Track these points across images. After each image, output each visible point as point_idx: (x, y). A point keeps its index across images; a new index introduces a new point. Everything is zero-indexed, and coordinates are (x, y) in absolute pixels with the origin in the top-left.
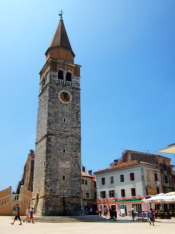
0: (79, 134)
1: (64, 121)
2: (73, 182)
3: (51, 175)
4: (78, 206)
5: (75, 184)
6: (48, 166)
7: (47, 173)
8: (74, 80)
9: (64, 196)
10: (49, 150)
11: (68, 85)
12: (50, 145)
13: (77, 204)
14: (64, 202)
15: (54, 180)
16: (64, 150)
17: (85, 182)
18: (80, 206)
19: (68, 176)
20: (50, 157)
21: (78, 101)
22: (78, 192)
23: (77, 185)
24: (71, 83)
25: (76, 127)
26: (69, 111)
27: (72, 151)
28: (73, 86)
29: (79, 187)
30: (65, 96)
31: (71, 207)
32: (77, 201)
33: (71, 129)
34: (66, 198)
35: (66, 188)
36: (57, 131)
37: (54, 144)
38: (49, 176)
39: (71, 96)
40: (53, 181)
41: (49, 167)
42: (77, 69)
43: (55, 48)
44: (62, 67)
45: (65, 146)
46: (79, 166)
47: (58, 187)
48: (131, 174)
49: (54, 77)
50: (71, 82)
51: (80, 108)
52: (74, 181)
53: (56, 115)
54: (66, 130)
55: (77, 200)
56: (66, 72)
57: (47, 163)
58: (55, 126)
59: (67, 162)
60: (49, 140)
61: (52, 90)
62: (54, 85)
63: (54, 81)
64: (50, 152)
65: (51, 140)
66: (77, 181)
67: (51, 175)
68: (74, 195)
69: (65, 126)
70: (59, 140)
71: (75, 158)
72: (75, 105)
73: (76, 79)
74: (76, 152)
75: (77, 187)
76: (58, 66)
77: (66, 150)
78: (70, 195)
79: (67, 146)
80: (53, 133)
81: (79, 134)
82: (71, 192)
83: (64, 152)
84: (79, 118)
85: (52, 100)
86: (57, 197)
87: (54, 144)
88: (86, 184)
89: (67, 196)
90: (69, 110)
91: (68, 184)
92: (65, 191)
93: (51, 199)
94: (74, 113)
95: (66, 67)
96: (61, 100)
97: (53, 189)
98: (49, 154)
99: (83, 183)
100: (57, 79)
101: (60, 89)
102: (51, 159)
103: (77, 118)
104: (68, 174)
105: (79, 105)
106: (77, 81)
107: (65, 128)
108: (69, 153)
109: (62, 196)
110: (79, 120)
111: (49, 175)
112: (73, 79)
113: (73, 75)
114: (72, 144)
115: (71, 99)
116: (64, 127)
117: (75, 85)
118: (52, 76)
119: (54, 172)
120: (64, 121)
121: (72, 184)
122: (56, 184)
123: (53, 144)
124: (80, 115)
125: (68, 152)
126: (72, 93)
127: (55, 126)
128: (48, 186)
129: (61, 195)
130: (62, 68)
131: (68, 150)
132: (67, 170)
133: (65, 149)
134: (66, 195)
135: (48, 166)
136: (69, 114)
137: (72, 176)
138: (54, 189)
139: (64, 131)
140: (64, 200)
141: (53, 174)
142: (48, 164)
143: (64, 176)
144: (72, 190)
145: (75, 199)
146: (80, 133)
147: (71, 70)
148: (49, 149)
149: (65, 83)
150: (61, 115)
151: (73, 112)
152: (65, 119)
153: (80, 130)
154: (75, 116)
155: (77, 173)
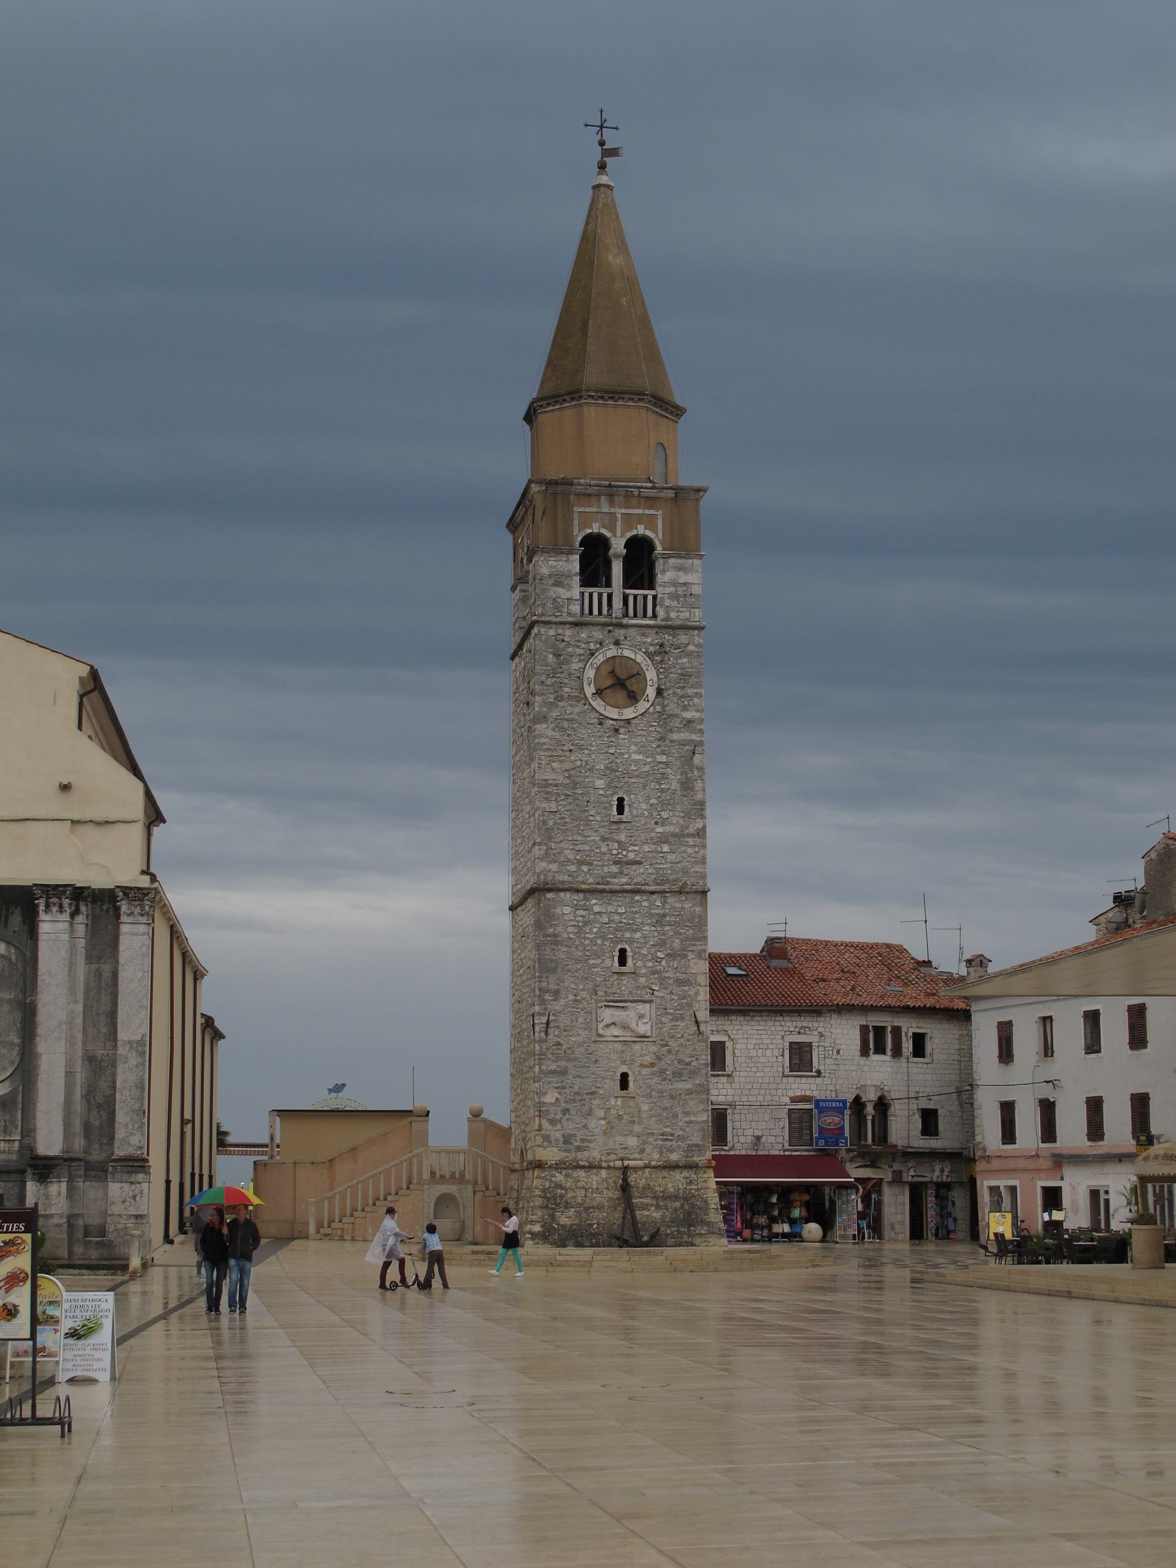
0: (698, 868)
1: (620, 810)
2: (666, 1103)
3: (563, 1072)
5: (679, 1110)
6: (547, 1034)
7: (544, 1067)
8: (669, 576)
9: (626, 1163)
10: (551, 961)
11: (635, 615)
12: (555, 936)
13: (741, 1195)
14: (625, 1188)
15: (578, 1094)
16: (623, 952)
17: (907, 1046)
19: (645, 1071)
21: (690, 691)
22: (697, 1145)
23: (686, 1114)
24: (655, 597)
25: (683, 836)
26: (641, 757)
27: (660, 955)
28: (661, 613)
29: (698, 1122)
31: (658, 1207)
32: (691, 1183)
33: (653, 847)
34: (636, 1169)
35: (638, 1129)
36: (585, 868)
37: (570, 929)
39: (651, 674)
40: (574, 1101)
43: (565, 400)
45: (628, 935)
46: (697, 1022)
47: (597, 1125)
48: (1131, 1008)
49: (558, 584)
52: (672, 1097)
53: (575, 785)
54: (631, 856)
55: (686, 1178)
56: (623, 542)
57: (544, 1020)
58: (575, 843)
62: (560, 631)
64: (554, 970)
65: (558, 911)
66: (689, 1092)
67: (563, 1072)
68: (674, 1157)
69: (622, 837)
70: (597, 909)
71: (678, 990)
72: (677, 716)
73: (680, 568)
75: (690, 1122)
76: (576, 516)
77: (629, 954)
78: (656, 1156)
79: (638, 935)
80: (566, 878)
81: (698, 868)
82: (661, 1143)
83: (623, 961)
84: (698, 785)
85: (554, 714)
87: (570, 929)
89: (640, 1163)
92: (632, 1142)
93: (567, 1175)
94: (667, 764)
95: (620, 511)
97: (574, 1135)
98: (552, 978)
99: (897, 1052)
100: (576, 591)
101: (592, 646)
102: (562, 1002)
103: (687, 786)
104: (642, 1065)
106: (683, 578)
108: (650, 964)
109: (618, 1164)
110: (699, 796)
111: (553, 1072)
112: (664, 571)
113: (659, 548)
114: (660, 920)
115: (651, 692)
116: (619, 842)
117: (675, 603)
118: (551, 582)
119: (575, 1059)
120: (620, 810)
121: (664, 1109)
122: (590, 1113)
125: (639, 964)
127: (575, 843)
128: (553, 1122)
129: (613, 1157)
130: (604, 526)
131: (644, 952)
132: (637, 1047)
133: (627, 947)
134: (637, 1156)
135: (547, 1034)
136: (647, 768)
137: (662, 1071)
139: (615, 863)
140: (625, 1180)
141: (572, 1072)
142: (548, 1023)
143: (624, 1076)
144: (663, 1135)
145: (679, 1176)
146: (703, 861)
147: (650, 522)
149: (617, 603)
150: (600, 783)
151: (663, 758)
155: (688, 1060)
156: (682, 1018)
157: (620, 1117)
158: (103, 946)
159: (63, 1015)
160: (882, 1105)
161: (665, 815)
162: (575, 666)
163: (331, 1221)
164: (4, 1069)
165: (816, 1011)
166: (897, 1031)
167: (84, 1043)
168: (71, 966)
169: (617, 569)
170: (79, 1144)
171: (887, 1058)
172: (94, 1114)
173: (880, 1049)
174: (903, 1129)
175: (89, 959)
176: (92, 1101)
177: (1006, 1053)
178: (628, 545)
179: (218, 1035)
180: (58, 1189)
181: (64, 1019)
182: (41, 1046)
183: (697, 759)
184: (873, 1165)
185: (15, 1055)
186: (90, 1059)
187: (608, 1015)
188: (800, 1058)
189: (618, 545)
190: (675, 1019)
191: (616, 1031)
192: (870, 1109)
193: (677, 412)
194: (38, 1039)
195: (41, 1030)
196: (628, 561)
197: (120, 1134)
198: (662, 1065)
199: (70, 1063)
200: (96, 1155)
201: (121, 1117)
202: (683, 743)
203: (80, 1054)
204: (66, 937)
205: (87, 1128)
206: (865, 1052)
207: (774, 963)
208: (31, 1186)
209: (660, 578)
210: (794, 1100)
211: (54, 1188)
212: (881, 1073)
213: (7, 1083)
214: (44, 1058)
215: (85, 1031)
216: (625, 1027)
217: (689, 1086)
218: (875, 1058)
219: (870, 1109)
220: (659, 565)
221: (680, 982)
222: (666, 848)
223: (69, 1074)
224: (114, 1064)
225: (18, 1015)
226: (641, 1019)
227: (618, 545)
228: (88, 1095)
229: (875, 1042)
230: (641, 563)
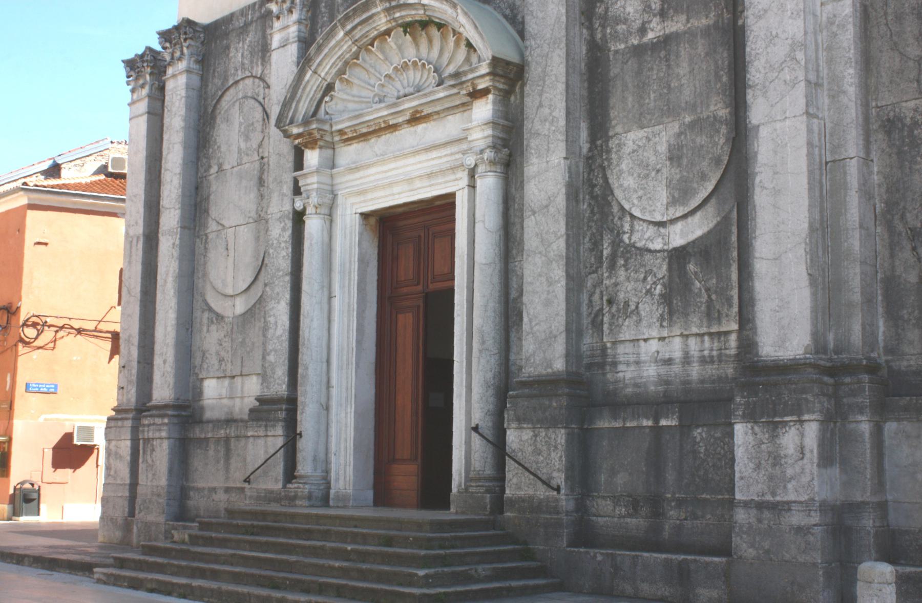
164: (704, 177)
167: (867, 90)
172: (906, 254)
176: (900, 227)
180: (802, 437)
181: (800, 36)
182: (758, 111)
194: (750, 92)
195: (756, 73)
203: (852, 113)
211: (789, 440)
213: (710, 208)
214: (764, 132)
215: (867, 63)
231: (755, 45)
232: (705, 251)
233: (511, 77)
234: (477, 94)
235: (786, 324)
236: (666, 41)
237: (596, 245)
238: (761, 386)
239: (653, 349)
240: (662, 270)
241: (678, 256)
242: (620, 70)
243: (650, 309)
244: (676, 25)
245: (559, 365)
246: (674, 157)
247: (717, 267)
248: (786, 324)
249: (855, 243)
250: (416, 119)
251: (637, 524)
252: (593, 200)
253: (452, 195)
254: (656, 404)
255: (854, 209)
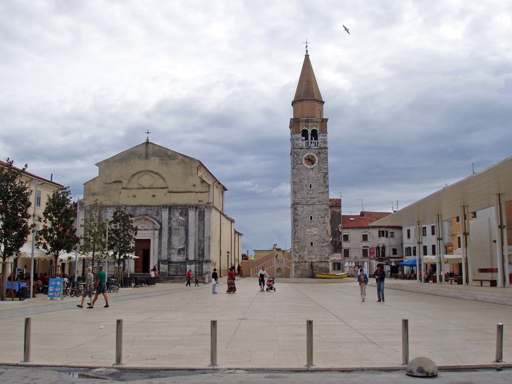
1: (311, 187)
4: (326, 269)
14: (312, 266)
16: (311, 217)
18: (329, 269)
20: (297, 226)
28: (319, 145)
30: (311, 160)
34: (314, 262)
38: (297, 243)
39: (317, 158)
41: (296, 235)
42: (324, 121)
44: (305, 126)
50: (317, 141)
51: (328, 170)
53: (301, 182)
56: (311, 131)
59: (315, 229)
60: (295, 209)
61: (295, 156)
63: (297, 145)
64: (297, 221)
66: (326, 246)
67: (299, 242)
68: (322, 260)
73: (323, 136)
74: (324, 217)
84: (327, 181)
85: (296, 167)
86: (306, 262)
88: (392, 236)
90: (315, 174)
91: (316, 249)
96: (306, 165)
99: (387, 236)
105: (326, 167)
106: (324, 138)
107: (311, 195)
115: (317, 162)
120: (311, 187)
122: (304, 250)
123: (299, 213)
124: (328, 178)
126: (318, 154)
128: (297, 252)
138: (302, 255)
145: (323, 263)
147: (317, 127)
148: (296, 218)
150: (306, 182)
152: (311, 185)
153: (328, 194)
154: (322, 181)
156: (324, 230)
157: (311, 251)
158: (201, 217)
159: (193, 232)
160: (384, 248)
161: (320, 188)
162: (301, 157)
163: (255, 273)
165: (369, 228)
166: (387, 232)
168: (196, 222)
169: (310, 136)
170: (197, 257)
171: (385, 238)
173: (383, 236)
174: (388, 253)
175: (199, 220)
177: (409, 237)
178: (312, 131)
179: (240, 234)
182: (189, 238)
183: (327, 176)
184: (381, 261)
185: (184, 240)
186: (199, 240)
187: (308, 230)
188: (365, 238)
189: (310, 132)
190: (322, 231)
191: (309, 233)
192: (381, 249)
193: (324, 102)
195: (189, 235)
196: (312, 135)
197: (205, 255)
198: (320, 240)
199: (195, 241)
200: (201, 259)
201: (205, 252)
202: (324, 172)
204: (194, 216)
205: (199, 254)
206: (380, 236)
207: (361, 217)
208: (188, 266)
209: (319, 138)
210: (363, 247)
212: (383, 241)
216: (312, 232)
217: (326, 245)
218: (382, 238)
219: (381, 249)
220: (318, 135)
221: (324, 223)
222: (320, 195)
223: (195, 244)
224: (204, 241)
225: (185, 232)
226: (315, 231)
227: (310, 132)
228: (199, 248)
229: (382, 234)
230: (315, 134)
231: (190, 231)
232: (183, 249)
233: (161, 229)
234: (156, 230)
235: (191, 257)
236: (178, 229)
237: (170, 247)
238: (187, 261)
239: (175, 258)
240: (178, 250)
241: (179, 250)
242: (173, 231)
243: (176, 254)
244: (180, 227)
245: (166, 259)
246: (179, 240)
247: (183, 251)
248: (191, 257)
249: (197, 250)
250: (145, 230)
251: (175, 274)
252: (170, 242)
253: (150, 240)
254: (177, 263)
255: (197, 247)
